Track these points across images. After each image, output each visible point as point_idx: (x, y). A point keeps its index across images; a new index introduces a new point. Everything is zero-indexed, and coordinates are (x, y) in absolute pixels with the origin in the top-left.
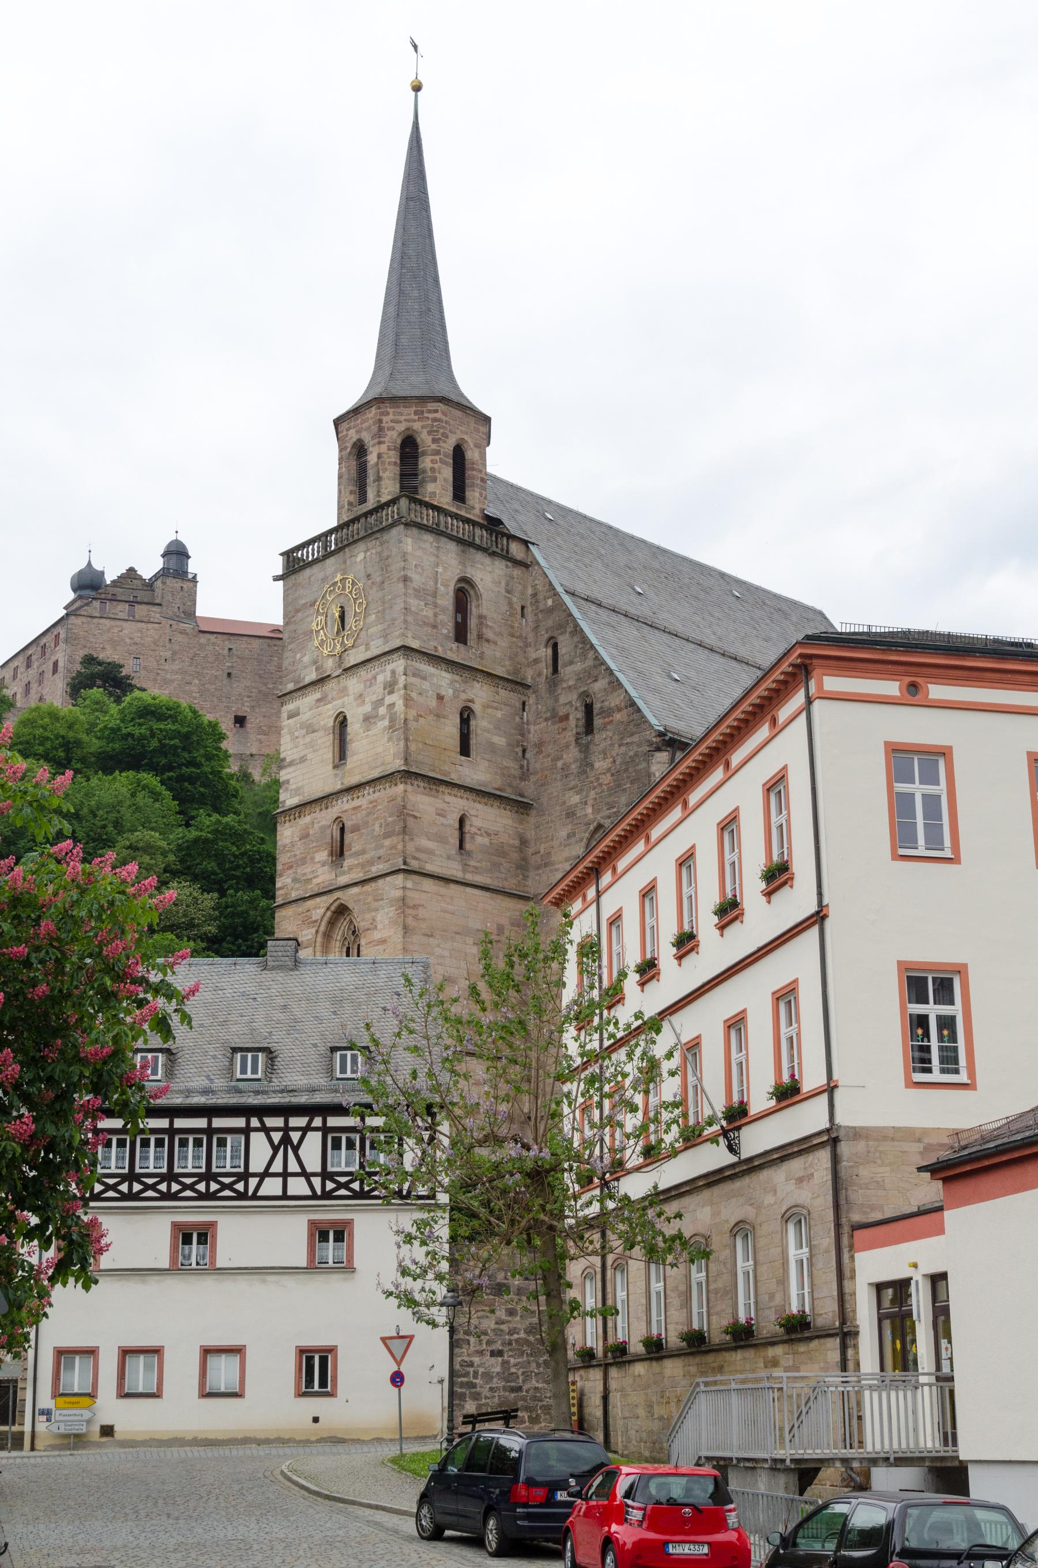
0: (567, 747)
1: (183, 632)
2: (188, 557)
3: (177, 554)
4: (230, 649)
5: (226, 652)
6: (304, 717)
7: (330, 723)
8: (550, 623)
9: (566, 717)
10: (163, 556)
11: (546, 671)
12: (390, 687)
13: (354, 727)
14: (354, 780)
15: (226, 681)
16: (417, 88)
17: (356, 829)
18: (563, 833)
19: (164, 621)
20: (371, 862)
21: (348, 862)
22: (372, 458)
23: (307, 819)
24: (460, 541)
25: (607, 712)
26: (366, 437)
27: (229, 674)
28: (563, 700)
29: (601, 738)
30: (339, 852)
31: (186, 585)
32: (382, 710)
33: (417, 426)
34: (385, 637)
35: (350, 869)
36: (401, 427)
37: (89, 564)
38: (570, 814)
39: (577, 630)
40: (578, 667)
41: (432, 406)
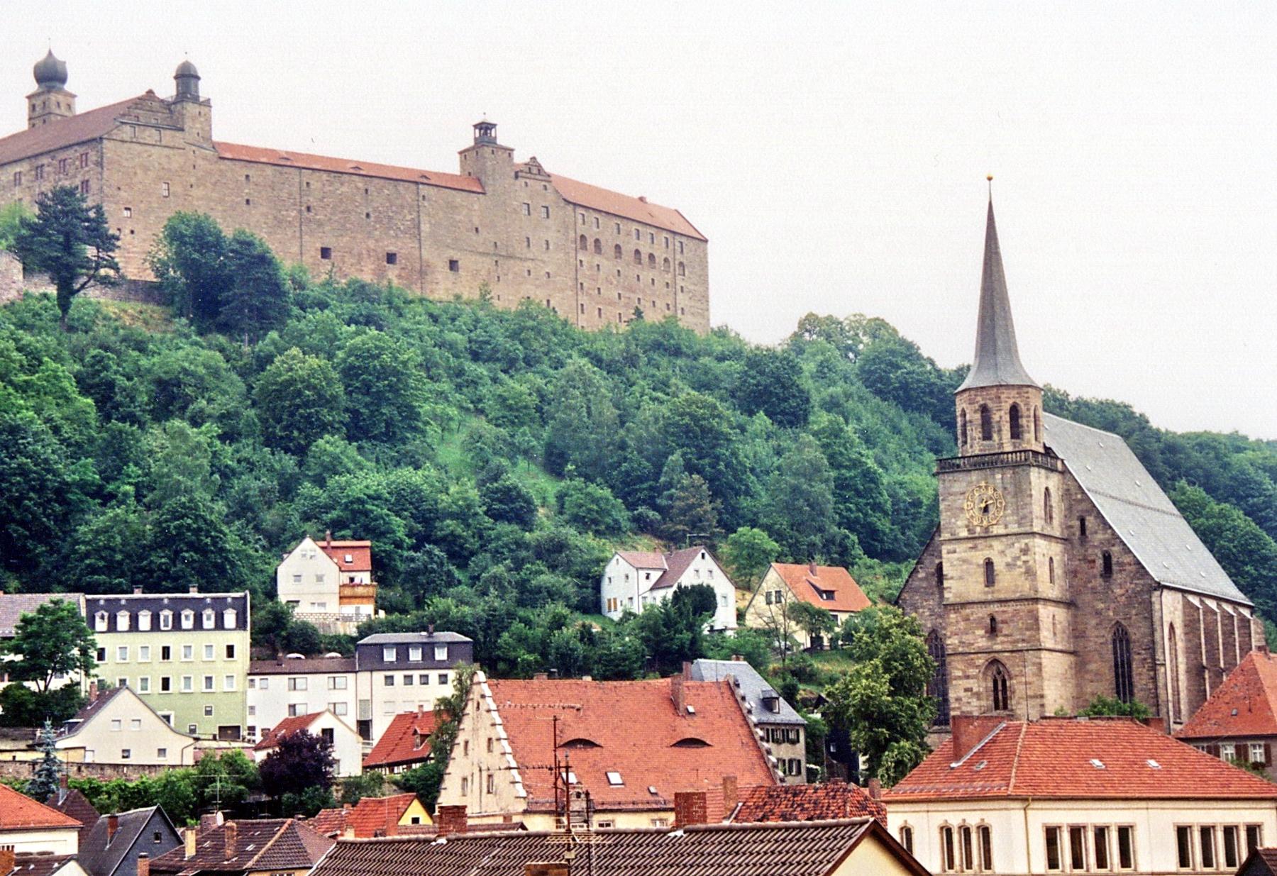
0: (1095, 577)
1: (205, 158)
2: (198, 78)
3: (187, 77)
4: (247, 176)
5: (243, 178)
6: (964, 555)
7: (981, 562)
8: (1080, 508)
9: (1094, 561)
10: (176, 78)
11: (1078, 533)
12: (1025, 551)
13: (999, 565)
14: (1002, 596)
15: (245, 207)
16: (990, 179)
17: (1004, 622)
18: (1094, 622)
19: (188, 147)
20: (1016, 641)
21: (1000, 639)
22: (996, 418)
23: (968, 611)
24: (1047, 469)
25: (1120, 564)
26: (990, 404)
27: (248, 202)
28: (1090, 551)
29: (1118, 577)
30: (993, 630)
31: (204, 110)
32: (1019, 563)
33: (1018, 401)
34: (1020, 525)
35: (1003, 643)
36: (1011, 401)
37: (50, 54)
38: (1098, 613)
39: (1099, 515)
40: (1100, 536)
41: (1025, 389)
